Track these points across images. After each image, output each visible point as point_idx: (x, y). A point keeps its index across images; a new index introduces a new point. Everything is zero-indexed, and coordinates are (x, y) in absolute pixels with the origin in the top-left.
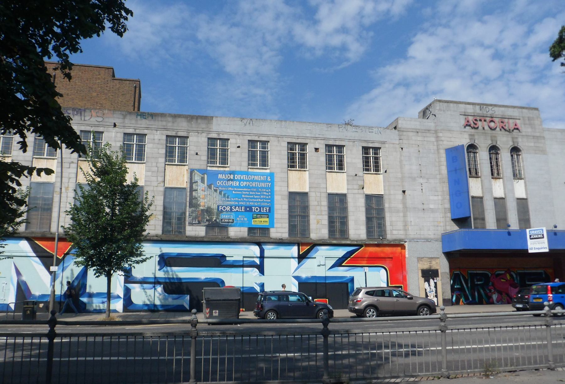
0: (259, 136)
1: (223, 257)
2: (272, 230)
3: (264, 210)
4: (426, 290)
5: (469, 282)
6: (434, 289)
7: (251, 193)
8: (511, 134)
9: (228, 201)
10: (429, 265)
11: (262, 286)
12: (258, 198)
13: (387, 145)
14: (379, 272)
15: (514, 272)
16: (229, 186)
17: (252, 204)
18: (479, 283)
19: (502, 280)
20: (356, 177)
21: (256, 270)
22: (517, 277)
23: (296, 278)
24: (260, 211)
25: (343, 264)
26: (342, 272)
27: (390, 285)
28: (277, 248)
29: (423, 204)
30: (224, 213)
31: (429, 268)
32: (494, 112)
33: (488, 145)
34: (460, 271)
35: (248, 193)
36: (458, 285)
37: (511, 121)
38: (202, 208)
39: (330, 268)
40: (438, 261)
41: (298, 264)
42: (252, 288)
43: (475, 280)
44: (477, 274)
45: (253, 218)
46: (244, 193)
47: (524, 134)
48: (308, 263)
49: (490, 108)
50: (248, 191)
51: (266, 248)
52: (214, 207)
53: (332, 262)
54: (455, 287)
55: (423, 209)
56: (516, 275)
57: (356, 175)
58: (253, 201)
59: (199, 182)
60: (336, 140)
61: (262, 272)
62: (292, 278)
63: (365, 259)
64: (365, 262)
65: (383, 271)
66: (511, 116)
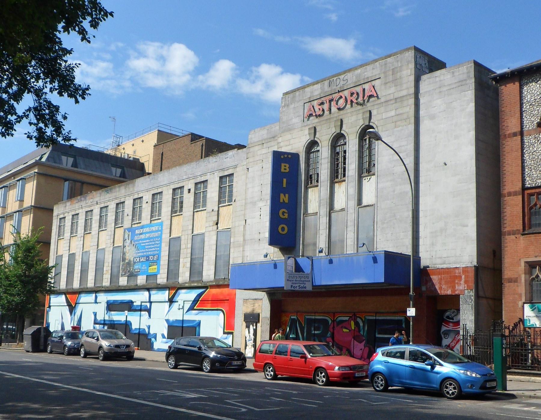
0: (157, 189)
1: (132, 302)
2: (159, 276)
3: (156, 257)
4: (246, 337)
5: (305, 331)
6: (252, 337)
7: (151, 243)
8: (364, 106)
9: (139, 253)
10: (252, 308)
11: (149, 327)
12: (153, 248)
13: (238, 169)
14: (218, 315)
15: (360, 318)
16: (140, 240)
17: (150, 253)
18: (316, 332)
19: (345, 330)
20: (213, 212)
21: (147, 313)
22: (364, 326)
23: (167, 321)
24: (153, 260)
25: (195, 308)
26: (193, 316)
27: (225, 331)
28: (158, 293)
29: (260, 233)
30: (136, 263)
31: (252, 312)
32: (346, 81)
33: (331, 135)
34: (297, 316)
35: (148, 244)
36: (293, 334)
37: (366, 86)
38: (127, 261)
39: (186, 313)
40: (260, 303)
41: (169, 307)
42: (144, 329)
43: (313, 329)
44: (315, 321)
45: (150, 267)
46: (147, 244)
47: (383, 100)
48: (175, 306)
49: (342, 77)
50: (149, 242)
51: (152, 292)
52: (132, 259)
53: (187, 306)
54: (291, 336)
55: (259, 240)
56: (363, 322)
57: (213, 210)
58: (148, 251)
59: (127, 239)
60: (202, 175)
61: (150, 316)
62: (165, 321)
63: (210, 302)
64: (209, 305)
65: (222, 314)
66: (368, 78)
